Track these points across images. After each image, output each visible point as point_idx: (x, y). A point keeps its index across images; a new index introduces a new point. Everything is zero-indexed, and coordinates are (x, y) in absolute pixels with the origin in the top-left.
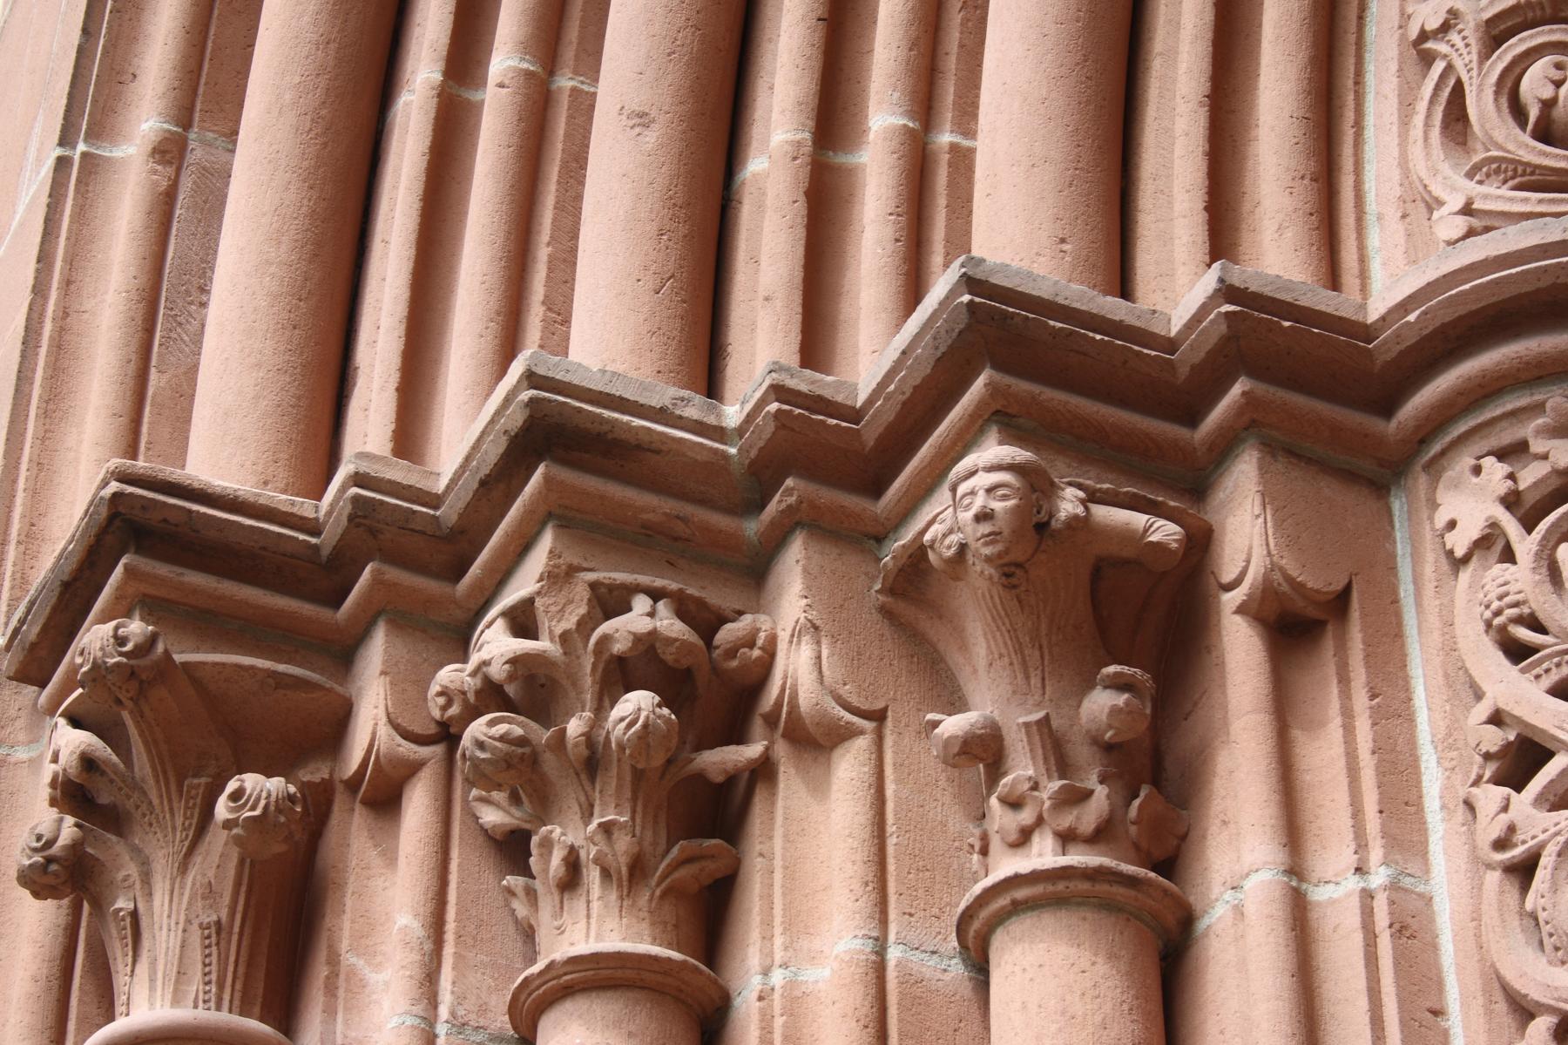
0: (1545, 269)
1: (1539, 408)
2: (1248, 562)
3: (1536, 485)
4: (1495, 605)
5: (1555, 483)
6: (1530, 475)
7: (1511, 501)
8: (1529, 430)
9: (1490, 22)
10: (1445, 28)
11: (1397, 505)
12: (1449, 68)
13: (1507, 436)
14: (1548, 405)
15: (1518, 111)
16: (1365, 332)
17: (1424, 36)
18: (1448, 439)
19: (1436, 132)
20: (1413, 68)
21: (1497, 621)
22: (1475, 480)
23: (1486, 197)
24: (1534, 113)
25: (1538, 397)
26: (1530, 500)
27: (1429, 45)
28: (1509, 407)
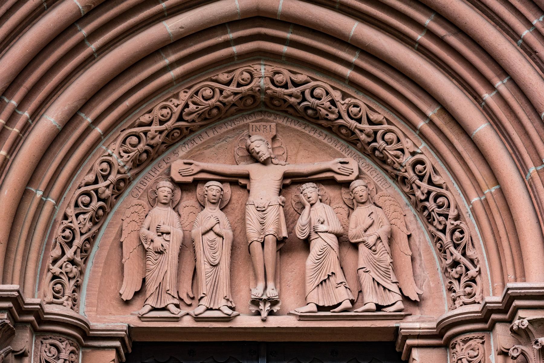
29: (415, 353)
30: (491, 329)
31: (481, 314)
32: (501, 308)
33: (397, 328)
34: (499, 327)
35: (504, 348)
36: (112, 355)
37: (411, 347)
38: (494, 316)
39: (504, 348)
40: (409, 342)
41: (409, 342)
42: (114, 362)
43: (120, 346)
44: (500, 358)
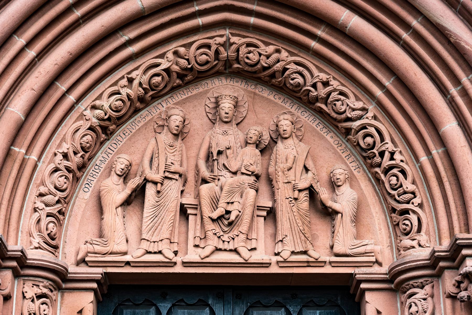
0: (54, 267)
1: (43, 282)
2: (6, 289)
3: (39, 293)
4: (31, 310)
5: (41, 294)
6: (39, 291)
7: (36, 294)
8: (41, 284)
9: (47, 213)
10: (41, 210)
11: (16, 282)
12: (40, 216)
13: (37, 283)
14: (44, 283)
15: (47, 229)
16: (26, 259)
17: (37, 208)
18: (29, 279)
19: (35, 225)
20: (33, 211)
21: (31, 312)
22: (32, 288)
23: (41, 242)
24: (49, 232)
25: (43, 281)
26: (37, 295)
27: (37, 209)
28: (40, 280)
29: (368, 296)
30: (439, 275)
31: (429, 262)
32: (448, 256)
33: (351, 274)
34: (447, 274)
35: (452, 293)
36: (90, 296)
37: (364, 290)
38: (442, 264)
39: (452, 293)
40: (363, 286)
41: (363, 286)
42: (93, 304)
43: (97, 288)
44: (448, 302)
